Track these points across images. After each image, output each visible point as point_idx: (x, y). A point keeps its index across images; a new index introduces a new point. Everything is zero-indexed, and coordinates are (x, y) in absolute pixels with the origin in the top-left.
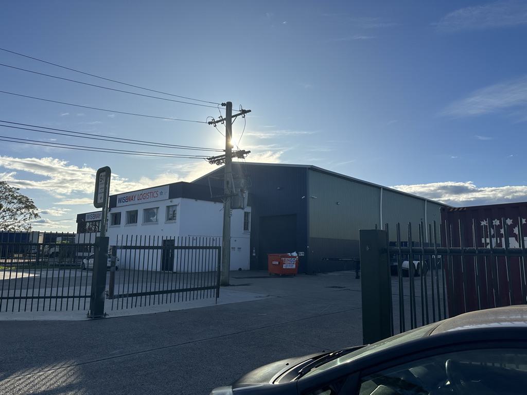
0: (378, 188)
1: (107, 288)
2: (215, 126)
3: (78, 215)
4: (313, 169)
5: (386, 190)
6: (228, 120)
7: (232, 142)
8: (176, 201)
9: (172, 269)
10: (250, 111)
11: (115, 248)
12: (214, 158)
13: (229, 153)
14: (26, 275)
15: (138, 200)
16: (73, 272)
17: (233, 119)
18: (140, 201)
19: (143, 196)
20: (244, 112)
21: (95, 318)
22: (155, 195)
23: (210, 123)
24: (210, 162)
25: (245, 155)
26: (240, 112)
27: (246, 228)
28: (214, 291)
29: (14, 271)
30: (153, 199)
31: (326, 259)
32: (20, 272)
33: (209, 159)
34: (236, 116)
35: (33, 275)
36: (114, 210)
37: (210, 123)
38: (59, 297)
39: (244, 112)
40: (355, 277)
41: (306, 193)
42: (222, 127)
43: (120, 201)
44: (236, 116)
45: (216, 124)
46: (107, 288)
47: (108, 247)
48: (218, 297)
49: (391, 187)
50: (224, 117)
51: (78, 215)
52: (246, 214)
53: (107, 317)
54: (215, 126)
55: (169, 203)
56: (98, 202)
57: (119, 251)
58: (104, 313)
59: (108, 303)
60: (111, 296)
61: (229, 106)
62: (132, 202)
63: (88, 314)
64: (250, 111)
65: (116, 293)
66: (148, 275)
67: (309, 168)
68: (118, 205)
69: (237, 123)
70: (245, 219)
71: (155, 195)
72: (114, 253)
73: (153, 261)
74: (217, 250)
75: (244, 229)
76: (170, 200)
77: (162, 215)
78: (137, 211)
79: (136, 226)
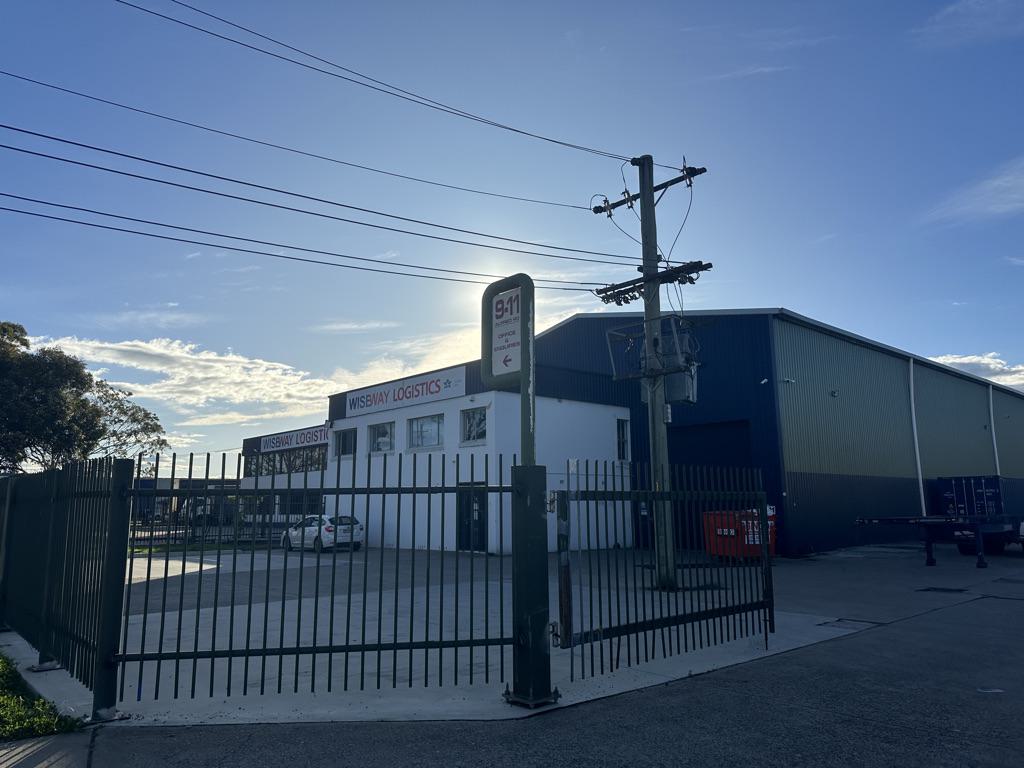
0: (904, 357)
1: (554, 616)
2: (610, 216)
3: (245, 440)
4: (783, 316)
5: (922, 363)
6: (647, 194)
7: (663, 247)
8: (482, 399)
9: (482, 544)
10: (703, 170)
11: (564, 498)
12: (614, 287)
13: (653, 277)
14: (192, 567)
15: (395, 400)
16: (261, 557)
17: (657, 195)
18: (399, 403)
19: (405, 392)
20: (691, 172)
21: (537, 706)
22: (433, 388)
23: (598, 210)
24: (603, 298)
25: (694, 276)
26: (681, 174)
27: (622, 456)
28: (758, 615)
29: (158, 557)
30: (431, 397)
31: (870, 521)
32: (175, 558)
33: (599, 292)
34: (665, 186)
35: (205, 567)
36: (342, 425)
37: (598, 210)
38: (433, 645)
39: (691, 172)
40: (924, 562)
41: (768, 369)
42: (630, 218)
43: (353, 404)
44: (665, 186)
45: (637, 204)
46: (554, 616)
47: (545, 496)
48: (772, 630)
49: (941, 360)
50: (635, 190)
51: (245, 440)
52: (621, 424)
53: (563, 702)
54: (610, 216)
55: (467, 403)
56: (495, 373)
57: (573, 504)
58: (553, 690)
59: (560, 662)
60: (568, 640)
61: (645, 164)
62: (382, 406)
63: (507, 692)
64: (703, 170)
65: (576, 629)
66: (417, 564)
67: (775, 316)
68: (349, 412)
69: (666, 209)
70: (619, 437)
71: (433, 388)
72: (564, 514)
73: (439, 524)
74: (628, 504)
75: (619, 458)
76: (470, 397)
77: (453, 427)
78: (355, 431)
79: (484, 445)
